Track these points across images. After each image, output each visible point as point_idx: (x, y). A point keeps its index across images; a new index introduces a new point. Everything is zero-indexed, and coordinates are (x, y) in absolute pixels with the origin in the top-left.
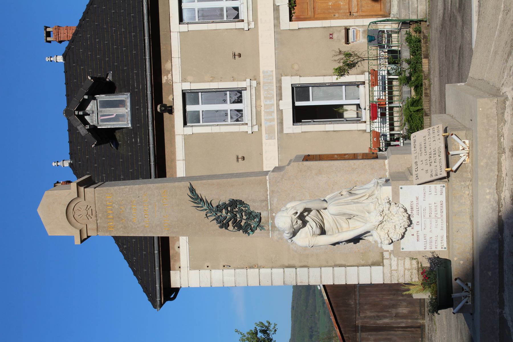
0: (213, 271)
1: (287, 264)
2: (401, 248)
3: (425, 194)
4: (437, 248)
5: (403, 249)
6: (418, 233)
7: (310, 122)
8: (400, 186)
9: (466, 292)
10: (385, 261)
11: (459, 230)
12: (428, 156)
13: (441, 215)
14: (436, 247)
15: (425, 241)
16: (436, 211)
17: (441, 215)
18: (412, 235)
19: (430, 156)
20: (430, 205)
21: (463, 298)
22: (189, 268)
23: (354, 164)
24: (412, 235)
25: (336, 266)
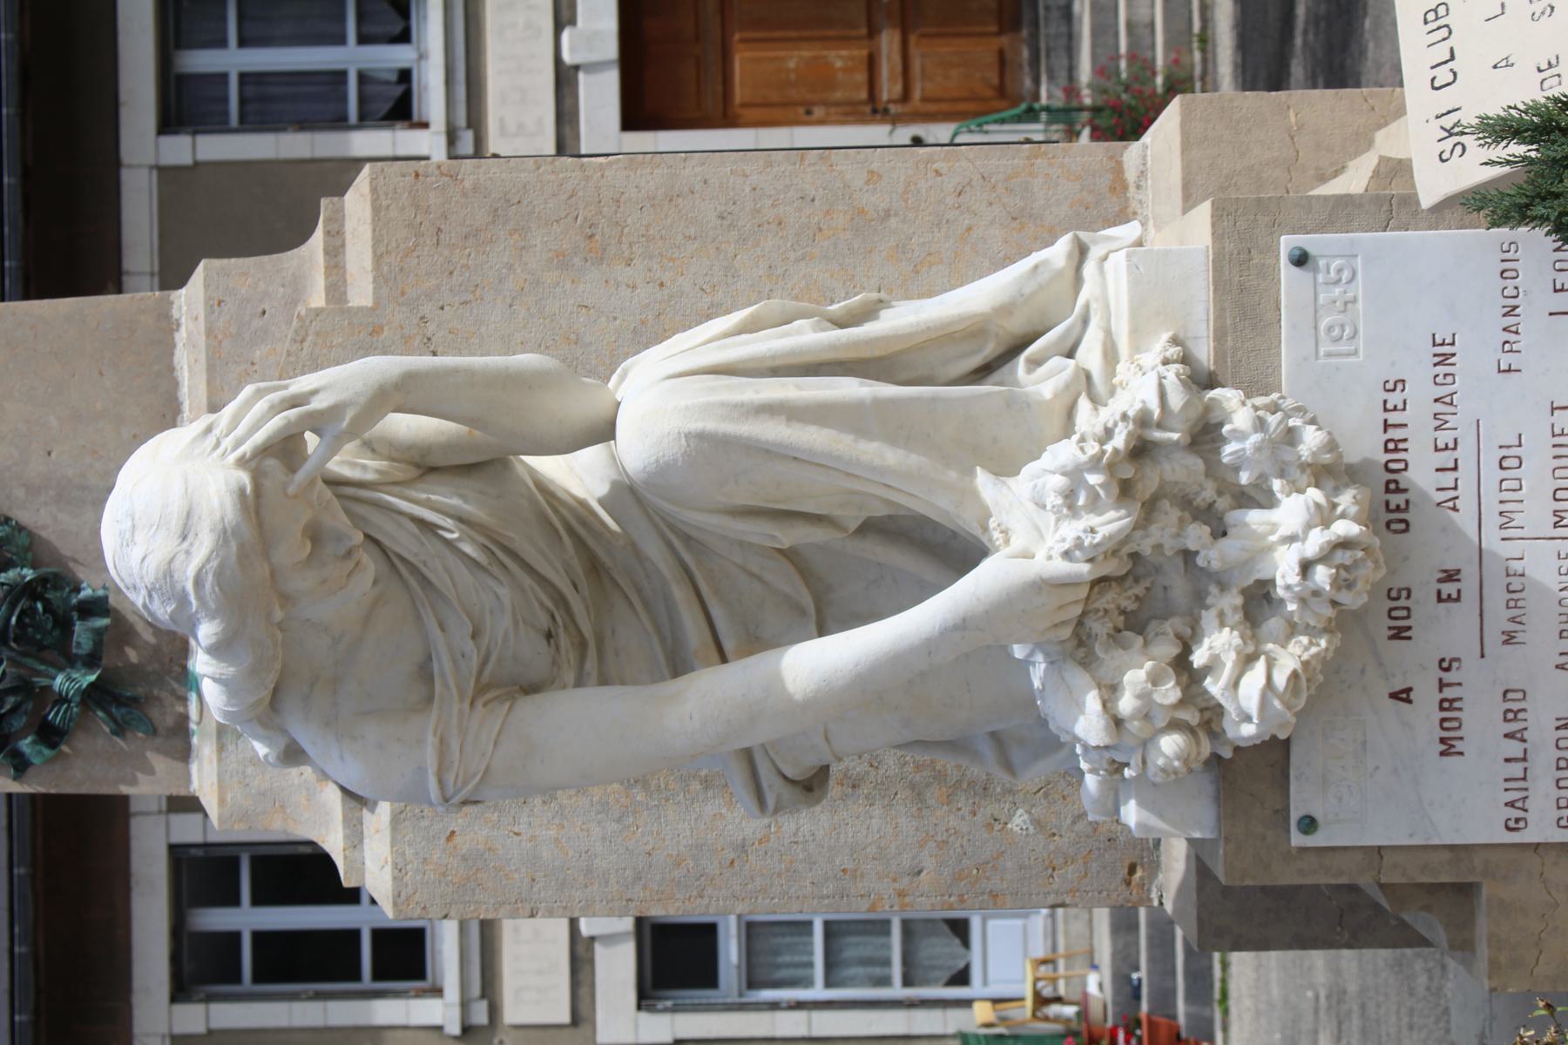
2: (1294, 816)
3: (1511, 311)
5: (1309, 824)
6: (1448, 677)
18: (1394, 696)
23: (873, 176)
24: (1394, 696)
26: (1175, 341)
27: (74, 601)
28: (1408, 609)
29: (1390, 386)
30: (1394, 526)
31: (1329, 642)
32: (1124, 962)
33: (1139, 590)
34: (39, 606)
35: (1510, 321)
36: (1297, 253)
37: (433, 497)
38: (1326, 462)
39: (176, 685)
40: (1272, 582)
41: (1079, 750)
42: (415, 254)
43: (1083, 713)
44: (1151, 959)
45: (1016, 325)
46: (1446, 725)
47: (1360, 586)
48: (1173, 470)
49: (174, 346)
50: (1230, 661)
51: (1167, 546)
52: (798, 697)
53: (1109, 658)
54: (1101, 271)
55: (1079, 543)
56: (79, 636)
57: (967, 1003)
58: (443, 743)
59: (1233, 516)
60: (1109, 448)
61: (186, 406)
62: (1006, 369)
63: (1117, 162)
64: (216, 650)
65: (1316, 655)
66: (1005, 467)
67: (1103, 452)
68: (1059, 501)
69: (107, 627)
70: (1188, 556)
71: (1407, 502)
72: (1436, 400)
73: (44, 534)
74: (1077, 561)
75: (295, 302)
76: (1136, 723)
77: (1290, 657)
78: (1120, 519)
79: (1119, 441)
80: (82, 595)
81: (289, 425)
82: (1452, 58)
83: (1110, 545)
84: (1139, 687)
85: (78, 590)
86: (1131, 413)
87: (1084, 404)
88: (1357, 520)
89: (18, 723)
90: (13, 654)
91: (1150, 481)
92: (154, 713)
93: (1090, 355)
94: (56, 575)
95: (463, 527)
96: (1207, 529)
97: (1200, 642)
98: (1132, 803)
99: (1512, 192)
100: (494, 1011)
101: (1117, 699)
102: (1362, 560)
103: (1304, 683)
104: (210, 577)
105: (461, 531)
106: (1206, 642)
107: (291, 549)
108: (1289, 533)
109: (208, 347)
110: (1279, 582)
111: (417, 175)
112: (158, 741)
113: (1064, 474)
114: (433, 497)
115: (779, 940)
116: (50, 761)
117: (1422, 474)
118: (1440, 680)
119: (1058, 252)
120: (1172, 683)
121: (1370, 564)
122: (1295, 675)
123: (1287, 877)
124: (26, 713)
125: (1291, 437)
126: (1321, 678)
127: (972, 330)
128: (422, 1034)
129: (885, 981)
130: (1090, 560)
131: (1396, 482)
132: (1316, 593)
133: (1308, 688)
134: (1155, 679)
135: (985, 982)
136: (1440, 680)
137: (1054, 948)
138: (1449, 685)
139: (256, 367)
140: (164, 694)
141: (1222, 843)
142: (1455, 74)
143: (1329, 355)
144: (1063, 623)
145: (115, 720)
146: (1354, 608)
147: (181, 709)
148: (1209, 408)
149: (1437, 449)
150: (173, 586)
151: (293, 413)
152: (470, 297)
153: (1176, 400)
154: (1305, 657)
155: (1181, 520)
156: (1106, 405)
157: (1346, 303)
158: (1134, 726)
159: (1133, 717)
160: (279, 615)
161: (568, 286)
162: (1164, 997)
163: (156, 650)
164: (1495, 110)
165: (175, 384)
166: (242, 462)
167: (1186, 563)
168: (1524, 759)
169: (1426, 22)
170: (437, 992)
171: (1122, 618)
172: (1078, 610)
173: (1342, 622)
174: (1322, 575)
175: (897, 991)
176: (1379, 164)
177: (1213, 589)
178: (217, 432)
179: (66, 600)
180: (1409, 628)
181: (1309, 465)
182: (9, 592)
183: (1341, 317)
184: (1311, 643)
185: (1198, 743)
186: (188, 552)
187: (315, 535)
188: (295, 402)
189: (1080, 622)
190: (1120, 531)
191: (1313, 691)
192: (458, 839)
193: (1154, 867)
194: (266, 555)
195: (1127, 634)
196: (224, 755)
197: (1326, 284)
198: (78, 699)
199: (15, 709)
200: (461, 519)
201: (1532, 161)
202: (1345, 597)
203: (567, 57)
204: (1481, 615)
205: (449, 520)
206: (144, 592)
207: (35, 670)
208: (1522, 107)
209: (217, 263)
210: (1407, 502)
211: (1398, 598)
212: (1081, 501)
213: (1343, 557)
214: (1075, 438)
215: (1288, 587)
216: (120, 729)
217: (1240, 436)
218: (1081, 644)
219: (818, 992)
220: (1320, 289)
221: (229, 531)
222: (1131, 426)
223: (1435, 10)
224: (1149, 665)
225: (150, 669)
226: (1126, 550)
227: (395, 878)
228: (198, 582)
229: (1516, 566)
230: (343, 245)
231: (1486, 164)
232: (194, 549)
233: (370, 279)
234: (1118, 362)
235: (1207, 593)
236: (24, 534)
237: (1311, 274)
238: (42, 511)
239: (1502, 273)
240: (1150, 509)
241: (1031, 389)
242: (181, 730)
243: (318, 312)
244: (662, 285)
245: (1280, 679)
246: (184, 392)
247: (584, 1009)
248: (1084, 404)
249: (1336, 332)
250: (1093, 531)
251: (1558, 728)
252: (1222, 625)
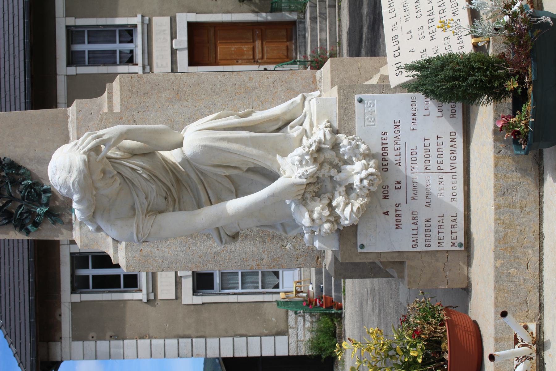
0: (98, 342)
1: (182, 335)
2: (359, 244)
4: (443, 244)
5: (362, 246)
6: (398, 209)
7: (173, 36)
8: (357, 97)
9: (523, 346)
10: (290, 330)
11: (507, 190)
12: (425, 18)
13: (452, 165)
14: (439, 243)
15: (414, 227)
16: (440, 156)
17: (452, 165)
18: (384, 213)
19: (431, 17)
20: (427, 142)
21: (516, 363)
22: (71, 339)
23: (251, 79)
24: (384, 213)
25: (236, 335)
26: (328, 122)
27: (42, 189)
28: (388, 191)
29: (383, 134)
30: (384, 170)
31: (367, 200)
32: (319, 282)
33: (319, 186)
34: (33, 190)
35: (414, 117)
36: (360, 99)
37: (135, 162)
38: (367, 153)
39: (69, 211)
40: (353, 184)
41: (303, 228)
42: (131, 98)
43: (304, 218)
44: (325, 281)
45: (287, 117)
46: (397, 221)
47: (375, 185)
48: (328, 155)
49: (68, 122)
50: (342, 204)
51: (326, 175)
52: (231, 214)
53: (311, 204)
54: (309, 103)
55: (303, 174)
56: (43, 198)
57: (278, 293)
58: (138, 226)
59: (343, 167)
60: (311, 149)
61: (71, 138)
62: (285, 129)
63: (314, 75)
64: (78, 202)
65: (365, 202)
66: (284, 154)
67: (310, 150)
68: (298, 163)
69: (50, 196)
70: (331, 177)
71: (388, 163)
72: (395, 137)
73: (34, 171)
74: (303, 179)
75: (100, 111)
76: (318, 221)
77: (357, 204)
78: (314, 168)
79: (314, 148)
80: (44, 187)
81: (97, 143)
82: (399, 49)
83: (311, 175)
84: (319, 211)
85: (43, 186)
86: (317, 140)
87: (305, 138)
88: (374, 168)
89: (27, 221)
90: (26, 203)
91: (322, 158)
92: (63, 218)
93: (306, 125)
94: (37, 182)
95: (143, 169)
96: (336, 170)
97: (334, 200)
98: (317, 241)
99: (413, 84)
100: (155, 296)
101: (313, 214)
102: (376, 178)
103: (361, 210)
104: (76, 183)
105: (142, 170)
106: (336, 199)
107: (97, 176)
108: (357, 171)
109: (77, 122)
110: (355, 184)
111: (132, 78)
112: (64, 226)
113: (299, 156)
114: (135, 162)
115: (230, 277)
116: (36, 231)
117: (391, 156)
118: (396, 209)
119: (298, 98)
120: (327, 210)
121: (378, 179)
122: (359, 208)
123: (357, 260)
124: (29, 219)
125: (358, 146)
126: (365, 209)
127: (276, 119)
128: (137, 302)
129: (257, 287)
130: (306, 179)
131: (385, 158)
132: (364, 187)
133: (362, 212)
134: (323, 209)
135: (283, 288)
136: (396, 209)
137: (301, 279)
138: (398, 211)
139: (89, 128)
140: (66, 214)
141: (340, 252)
142: (400, 53)
143: (368, 125)
144: (299, 195)
145: (53, 221)
146: (374, 191)
147: (70, 217)
148: (336, 139)
149: (395, 150)
150: (67, 185)
151: (98, 140)
152: (146, 110)
153: (328, 137)
154: (361, 203)
155: (329, 168)
156: (310, 138)
157: (372, 112)
158: (317, 221)
159: (317, 219)
160: (94, 193)
161: (171, 107)
162: (329, 291)
163: (64, 202)
164: (409, 63)
165: (68, 132)
166: (85, 153)
167: (331, 179)
168: (417, 230)
169: (392, 40)
170: (141, 291)
171: (314, 193)
172: (303, 191)
173: (371, 194)
174: (366, 182)
175: (260, 290)
176: (381, 76)
177: (338, 186)
178: (78, 145)
179: (40, 189)
180: (388, 196)
181: (362, 154)
182: (25, 187)
183: (371, 116)
184: (363, 200)
185: (334, 226)
186: (70, 176)
187: (104, 172)
188: (98, 137)
189: (304, 195)
190: (314, 171)
191: (363, 212)
192: (143, 251)
193: (324, 258)
194: (91, 177)
195: (316, 197)
196: (82, 229)
197: (367, 107)
198: (43, 215)
199: (26, 217)
200: (142, 168)
201: (418, 76)
202: (371, 188)
203: (174, 47)
204: (406, 193)
205: (140, 168)
206: (59, 187)
207: (31, 207)
208: (416, 62)
209: (79, 100)
210: (388, 163)
211: (385, 188)
212: (304, 163)
213: (371, 178)
214: (302, 147)
215: (357, 185)
216: (54, 223)
217: (345, 146)
218: (304, 200)
219: (240, 290)
220: (365, 108)
221: (81, 171)
222: (317, 144)
223: (395, 37)
224: (321, 205)
225: (62, 207)
226: (315, 176)
227: (126, 261)
228: (73, 184)
229: (415, 180)
230: (112, 96)
231: (407, 76)
232: (72, 176)
233: (120, 105)
234: (314, 127)
235: (336, 187)
236: (29, 171)
237: (363, 105)
238: (33, 165)
239: (412, 105)
240: (321, 165)
241: (291, 134)
242: (70, 223)
243: (106, 113)
244: (196, 107)
245: (355, 209)
246: (71, 134)
247: (179, 295)
248: (305, 138)
249: (370, 120)
250: (307, 171)
251: (425, 221)
252: (340, 195)
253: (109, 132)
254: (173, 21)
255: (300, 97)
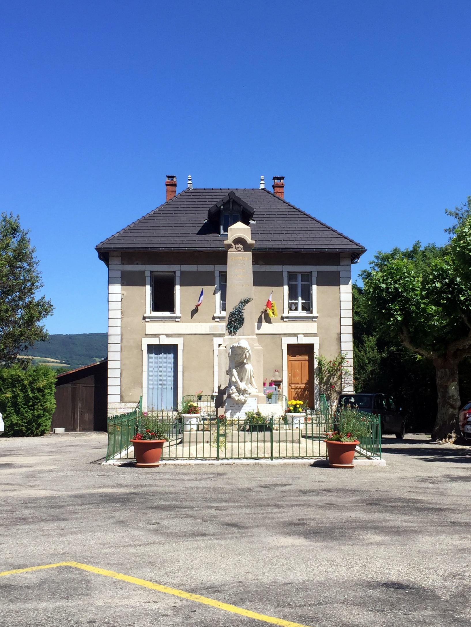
1: (123, 337)
10: (124, 404)
25: (121, 371)
203: (299, 336)
253: (250, 352)
254: (315, 335)
255: (256, 387)
